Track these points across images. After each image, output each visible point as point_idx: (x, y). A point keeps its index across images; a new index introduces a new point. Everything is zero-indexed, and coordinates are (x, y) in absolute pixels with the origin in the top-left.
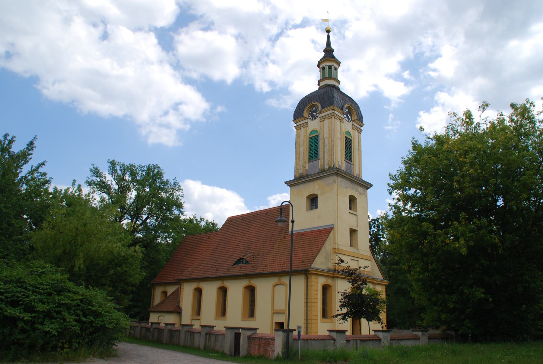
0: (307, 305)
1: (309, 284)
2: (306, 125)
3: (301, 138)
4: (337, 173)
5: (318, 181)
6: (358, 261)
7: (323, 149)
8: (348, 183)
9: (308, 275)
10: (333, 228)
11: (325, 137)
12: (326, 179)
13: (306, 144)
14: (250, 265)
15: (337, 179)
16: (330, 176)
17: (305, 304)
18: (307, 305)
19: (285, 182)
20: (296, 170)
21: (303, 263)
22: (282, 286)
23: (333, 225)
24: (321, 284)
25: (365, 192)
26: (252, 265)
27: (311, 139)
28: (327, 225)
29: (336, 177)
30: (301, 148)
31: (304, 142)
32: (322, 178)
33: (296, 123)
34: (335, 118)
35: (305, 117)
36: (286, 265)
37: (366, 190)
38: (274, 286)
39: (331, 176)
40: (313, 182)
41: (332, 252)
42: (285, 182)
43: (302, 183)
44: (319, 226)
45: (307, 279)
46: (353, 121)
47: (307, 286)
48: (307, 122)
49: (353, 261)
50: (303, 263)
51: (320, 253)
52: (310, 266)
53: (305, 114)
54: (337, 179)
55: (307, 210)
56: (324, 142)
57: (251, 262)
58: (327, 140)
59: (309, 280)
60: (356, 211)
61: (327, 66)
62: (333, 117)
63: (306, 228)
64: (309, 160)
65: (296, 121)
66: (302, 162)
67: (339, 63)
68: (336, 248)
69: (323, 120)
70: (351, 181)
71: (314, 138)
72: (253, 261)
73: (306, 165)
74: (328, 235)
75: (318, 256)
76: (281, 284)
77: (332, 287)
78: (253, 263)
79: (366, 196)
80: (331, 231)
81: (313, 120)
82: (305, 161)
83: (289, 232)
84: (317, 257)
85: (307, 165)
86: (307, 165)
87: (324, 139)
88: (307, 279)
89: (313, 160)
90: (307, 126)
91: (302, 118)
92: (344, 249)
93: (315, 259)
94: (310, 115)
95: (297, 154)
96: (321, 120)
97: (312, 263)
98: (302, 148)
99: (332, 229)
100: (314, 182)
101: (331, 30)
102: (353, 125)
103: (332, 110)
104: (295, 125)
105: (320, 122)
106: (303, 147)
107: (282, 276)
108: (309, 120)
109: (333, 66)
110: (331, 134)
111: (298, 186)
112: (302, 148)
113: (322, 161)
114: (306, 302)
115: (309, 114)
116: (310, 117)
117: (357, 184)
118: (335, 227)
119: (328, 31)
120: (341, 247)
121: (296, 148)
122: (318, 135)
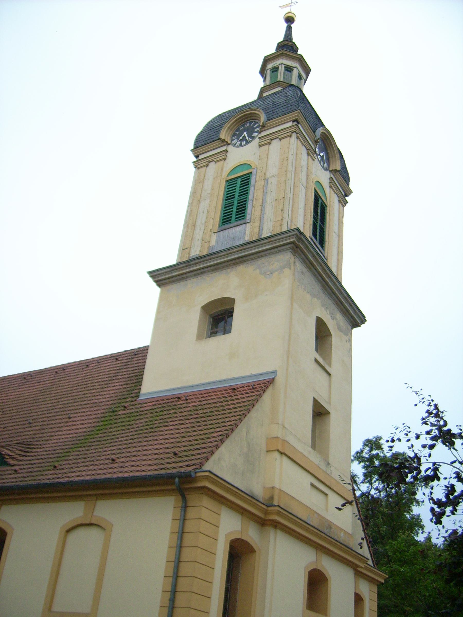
0: (173, 600)
1: (190, 526)
2: (225, 157)
3: (206, 183)
4: (298, 247)
5: (241, 268)
6: (326, 495)
7: (261, 200)
8: (317, 288)
9: (189, 497)
10: (273, 379)
11: (268, 175)
12: (262, 261)
13: (216, 195)
14: (9, 468)
15: (295, 262)
16: (274, 253)
17: (168, 596)
18: (173, 600)
19: (150, 273)
20: (183, 249)
21: (174, 460)
22: (93, 532)
23: (275, 372)
24: (227, 535)
25: (348, 329)
26: (14, 468)
27: (231, 183)
28: (254, 373)
29: (293, 258)
30: (202, 204)
31: (212, 189)
32: (253, 259)
33: (197, 157)
34: (298, 138)
35: (223, 141)
36: (116, 465)
37: (350, 327)
38: (69, 531)
39: (279, 252)
40: (224, 271)
41: (264, 448)
42: (150, 273)
43: (195, 275)
44: (229, 377)
45: (185, 507)
46: (331, 171)
47: (181, 533)
48: (226, 151)
49: (315, 492)
50: (174, 460)
51: (232, 436)
52: (201, 465)
53: (223, 135)
54: (295, 262)
55: (199, 337)
56: (265, 187)
57: (12, 462)
58: (273, 181)
59: (191, 513)
60: (330, 365)
61: (283, 66)
62: (294, 134)
63: (191, 384)
64: (219, 227)
65: (198, 150)
66: (201, 233)
67: (307, 71)
68: (278, 437)
69: (269, 141)
70: (323, 287)
71: (239, 180)
72: (21, 458)
73: (210, 236)
74: (260, 396)
75: (227, 443)
76: (91, 525)
77: (257, 554)
78: (20, 463)
79: (350, 341)
80: (267, 387)
81: (241, 145)
82: (210, 227)
83: (138, 396)
84: (224, 444)
85: (214, 237)
86: (214, 237)
87: (266, 180)
88: (185, 507)
89: (231, 225)
90: (225, 159)
91: (217, 143)
92: (299, 447)
93: (217, 447)
94: (235, 137)
95: (190, 216)
96: (261, 143)
97: (207, 459)
98: (205, 205)
99: (271, 382)
100: (229, 270)
101: (295, 18)
102: (331, 178)
103: (293, 121)
104: (195, 159)
105: (260, 146)
106: (207, 202)
107: (98, 497)
108: (230, 148)
109: (295, 69)
110: (287, 167)
111: (183, 283)
112: (205, 205)
113: (257, 224)
114: (169, 588)
115: (234, 135)
116: (236, 141)
117: (334, 300)
118: (280, 380)
119: (290, 20)
120: (292, 440)
121: (191, 204)
122: (251, 173)
